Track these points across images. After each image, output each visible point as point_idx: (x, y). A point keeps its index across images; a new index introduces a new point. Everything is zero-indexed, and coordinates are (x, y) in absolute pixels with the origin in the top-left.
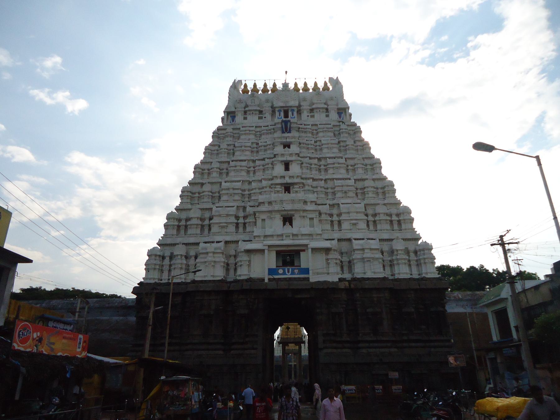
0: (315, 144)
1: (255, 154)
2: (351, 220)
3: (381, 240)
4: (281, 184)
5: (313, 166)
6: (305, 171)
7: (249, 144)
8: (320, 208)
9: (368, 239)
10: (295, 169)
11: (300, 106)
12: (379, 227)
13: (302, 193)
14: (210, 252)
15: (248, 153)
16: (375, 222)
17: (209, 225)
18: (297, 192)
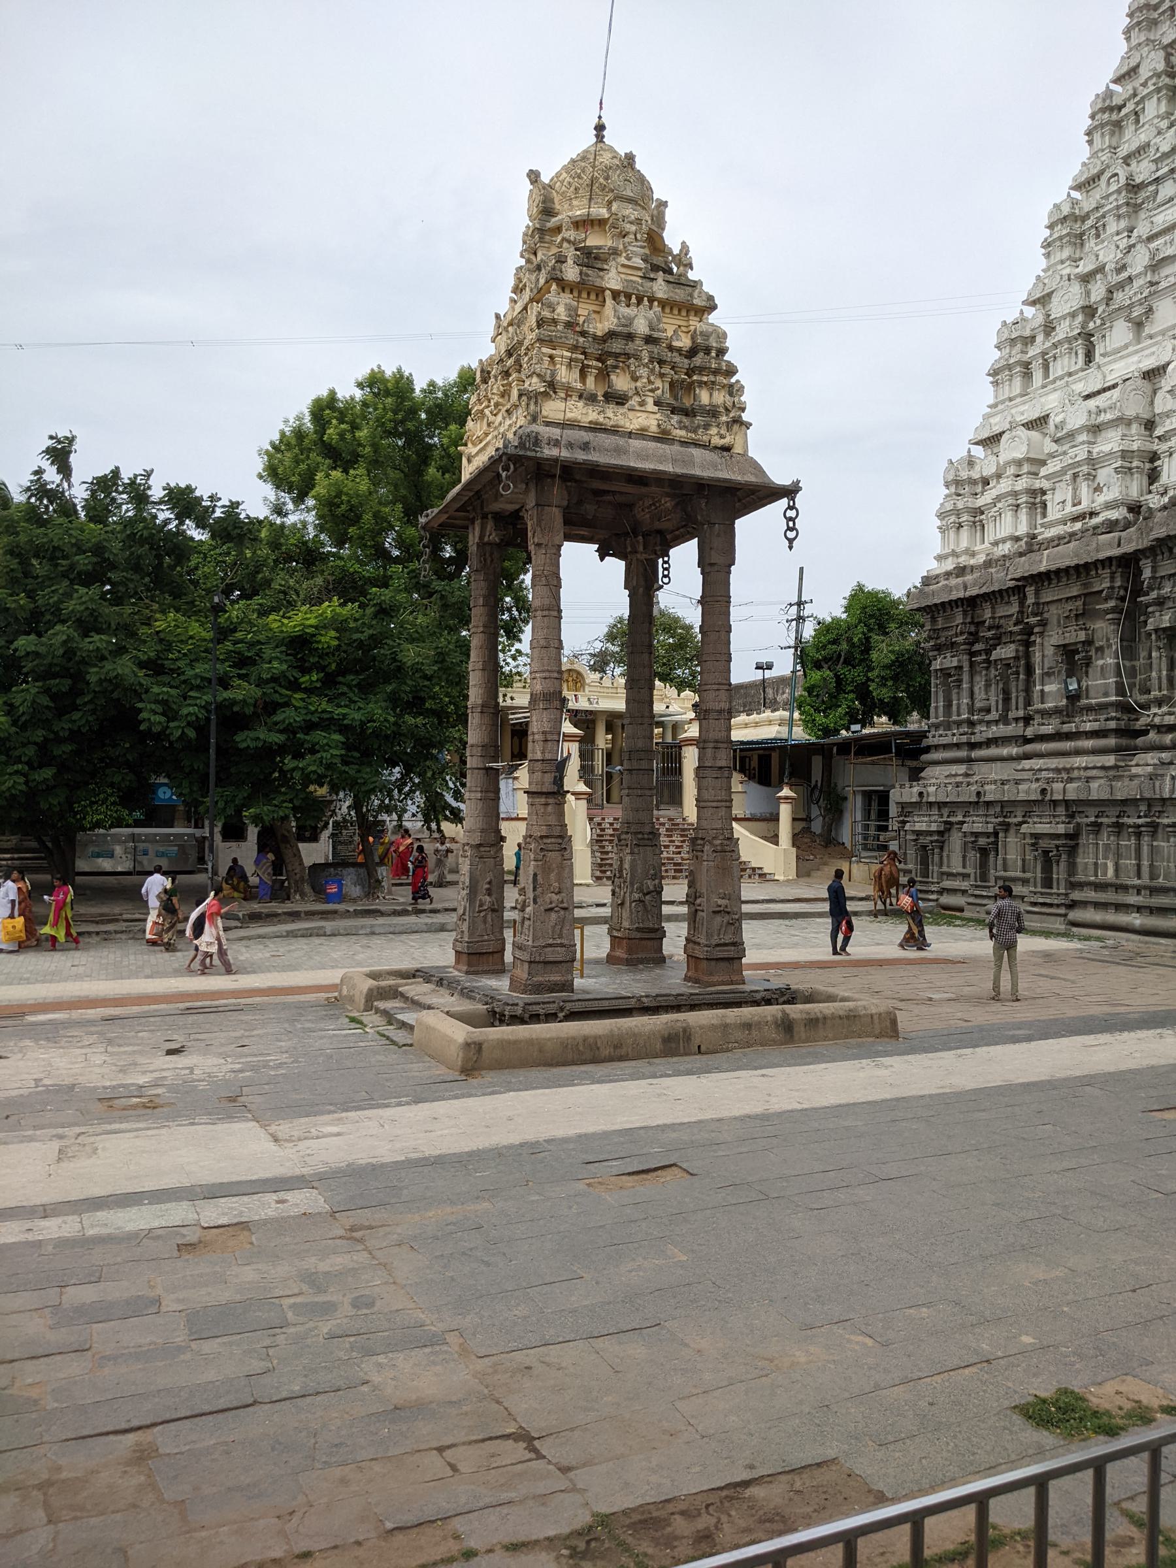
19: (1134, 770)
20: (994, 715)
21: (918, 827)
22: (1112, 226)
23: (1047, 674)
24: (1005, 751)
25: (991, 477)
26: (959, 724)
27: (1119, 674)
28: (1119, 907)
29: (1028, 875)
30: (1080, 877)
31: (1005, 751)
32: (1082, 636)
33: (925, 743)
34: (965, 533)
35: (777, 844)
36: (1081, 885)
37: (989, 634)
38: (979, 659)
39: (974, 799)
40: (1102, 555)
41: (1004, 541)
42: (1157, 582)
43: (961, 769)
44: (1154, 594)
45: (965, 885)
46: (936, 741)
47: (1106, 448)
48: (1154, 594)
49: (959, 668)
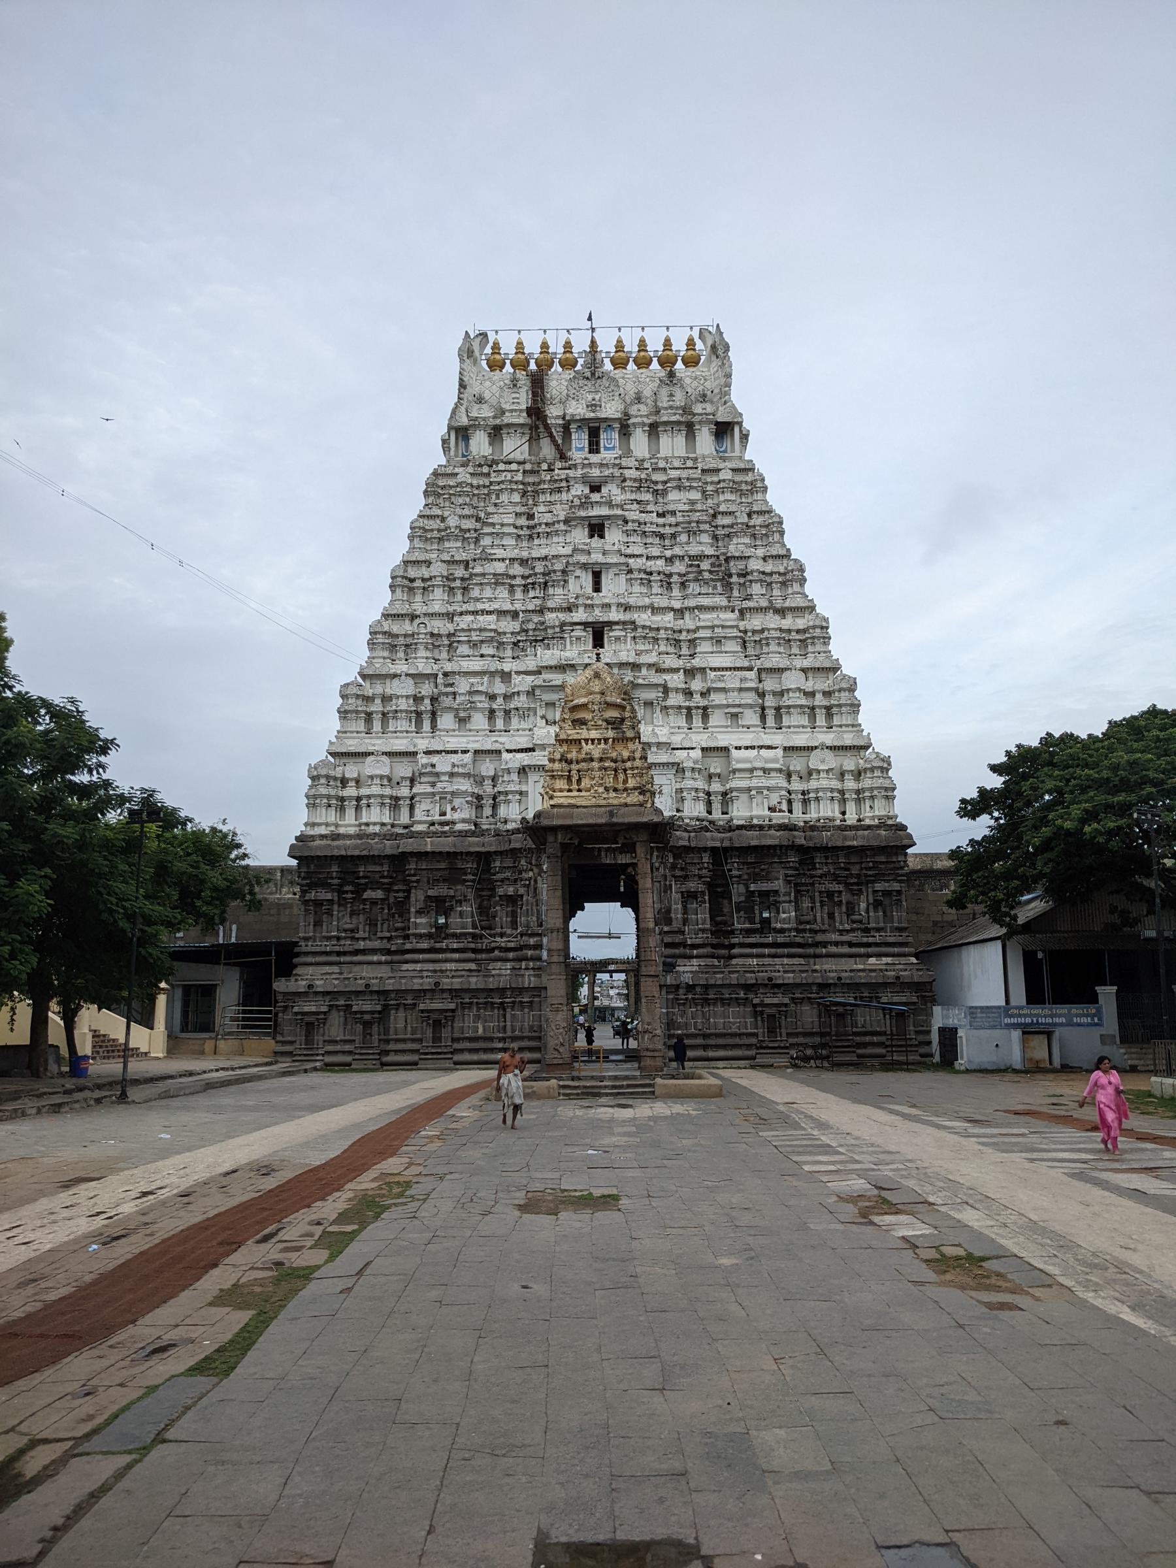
0: (661, 521)
1: (525, 544)
2: (728, 706)
3: (785, 749)
4: (585, 625)
5: (655, 577)
6: (637, 588)
7: (509, 519)
8: (667, 677)
9: (761, 747)
10: (613, 586)
11: (627, 415)
12: (786, 721)
13: (630, 644)
14: (444, 774)
15: (510, 541)
16: (778, 709)
17: (433, 714)
18: (618, 639)
19: (494, 972)
20: (361, 934)
21: (306, 1009)
22: (422, 653)
23: (419, 912)
24: (375, 958)
25: (352, 779)
26: (329, 938)
27: (473, 916)
28: (485, 1050)
29: (419, 1036)
30: (456, 1035)
31: (375, 958)
32: (452, 893)
33: (297, 950)
34: (332, 811)
35: (152, 1028)
36: (457, 1040)
37: (363, 881)
38: (350, 896)
39: (362, 989)
40: (472, 850)
41: (375, 824)
42: (503, 869)
43: (336, 969)
44: (499, 876)
45: (347, 1047)
46: (309, 949)
47: (463, 788)
48: (499, 876)
49: (331, 902)
